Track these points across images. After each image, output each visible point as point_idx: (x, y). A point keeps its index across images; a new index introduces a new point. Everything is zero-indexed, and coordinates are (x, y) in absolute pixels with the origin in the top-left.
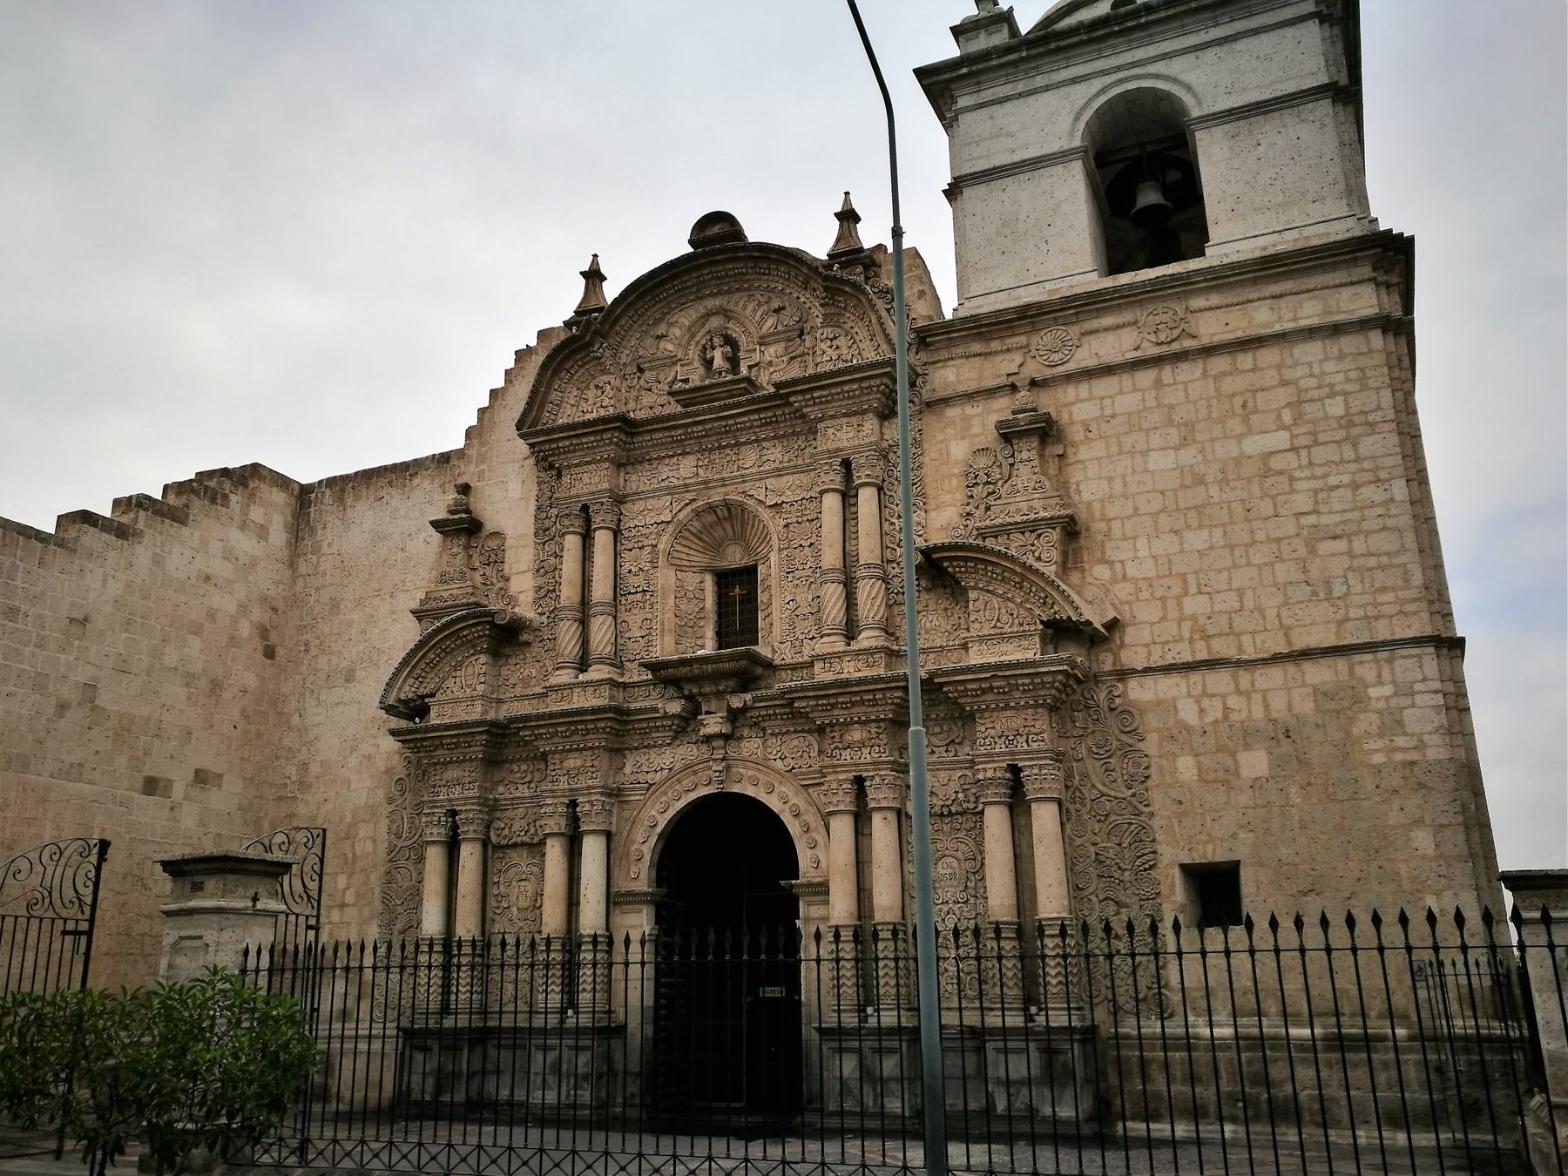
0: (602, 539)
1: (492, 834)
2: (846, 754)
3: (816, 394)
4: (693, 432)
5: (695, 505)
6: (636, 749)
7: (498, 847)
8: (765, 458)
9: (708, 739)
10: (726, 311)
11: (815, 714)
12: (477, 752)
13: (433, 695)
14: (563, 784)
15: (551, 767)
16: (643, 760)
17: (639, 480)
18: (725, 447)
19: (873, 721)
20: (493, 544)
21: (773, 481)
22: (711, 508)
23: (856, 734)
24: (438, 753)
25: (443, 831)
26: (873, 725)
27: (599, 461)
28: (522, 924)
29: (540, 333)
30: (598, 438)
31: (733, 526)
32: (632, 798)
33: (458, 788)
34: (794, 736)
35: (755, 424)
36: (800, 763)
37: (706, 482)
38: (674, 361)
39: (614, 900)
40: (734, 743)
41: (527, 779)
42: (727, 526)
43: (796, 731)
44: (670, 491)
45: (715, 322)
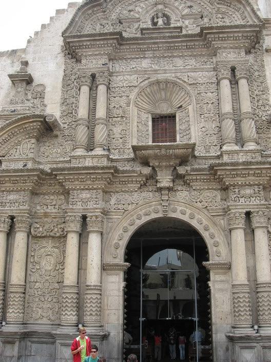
0: (102, 89)
1: (32, 230)
2: (242, 200)
3: (221, 36)
4: (152, 47)
5: (150, 80)
6: (117, 192)
7: (36, 237)
8: (187, 64)
9: (160, 189)
10: (165, 3)
11: (227, 179)
12: (29, 185)
13: (4, 157)
14: (79, 206)
15: (72, 197)
16: (121, 198)
17: (118, 66)
18: (166, 57)
19: (256, 185)
20: (39, 89)
21: (192, 74)
22: (158, 82)
23: (248, 191)
24: (7, 185)
25: (6, 226)
26: (256, 187)
27: (102, 55)
28: (48, 278)
29: (69, 4)
30: (105, 42)
31: (166, 94)
32: (114, 217)
33: (17, 204)
34: (207, 191)
35: (183, 47)
36: (211, 204)
37: (156, 70)
38: (138, 20)
39: (105, 268)
40: (174, 193)
41: (54, 203)
42: (163, 93)
43: (208, 189)
44: (136, 72)
45: (160, 7)
